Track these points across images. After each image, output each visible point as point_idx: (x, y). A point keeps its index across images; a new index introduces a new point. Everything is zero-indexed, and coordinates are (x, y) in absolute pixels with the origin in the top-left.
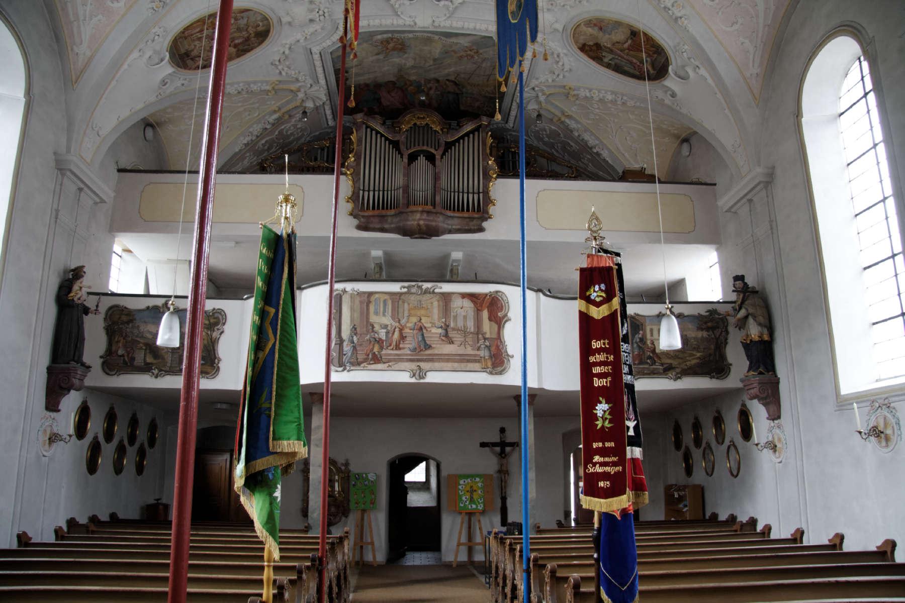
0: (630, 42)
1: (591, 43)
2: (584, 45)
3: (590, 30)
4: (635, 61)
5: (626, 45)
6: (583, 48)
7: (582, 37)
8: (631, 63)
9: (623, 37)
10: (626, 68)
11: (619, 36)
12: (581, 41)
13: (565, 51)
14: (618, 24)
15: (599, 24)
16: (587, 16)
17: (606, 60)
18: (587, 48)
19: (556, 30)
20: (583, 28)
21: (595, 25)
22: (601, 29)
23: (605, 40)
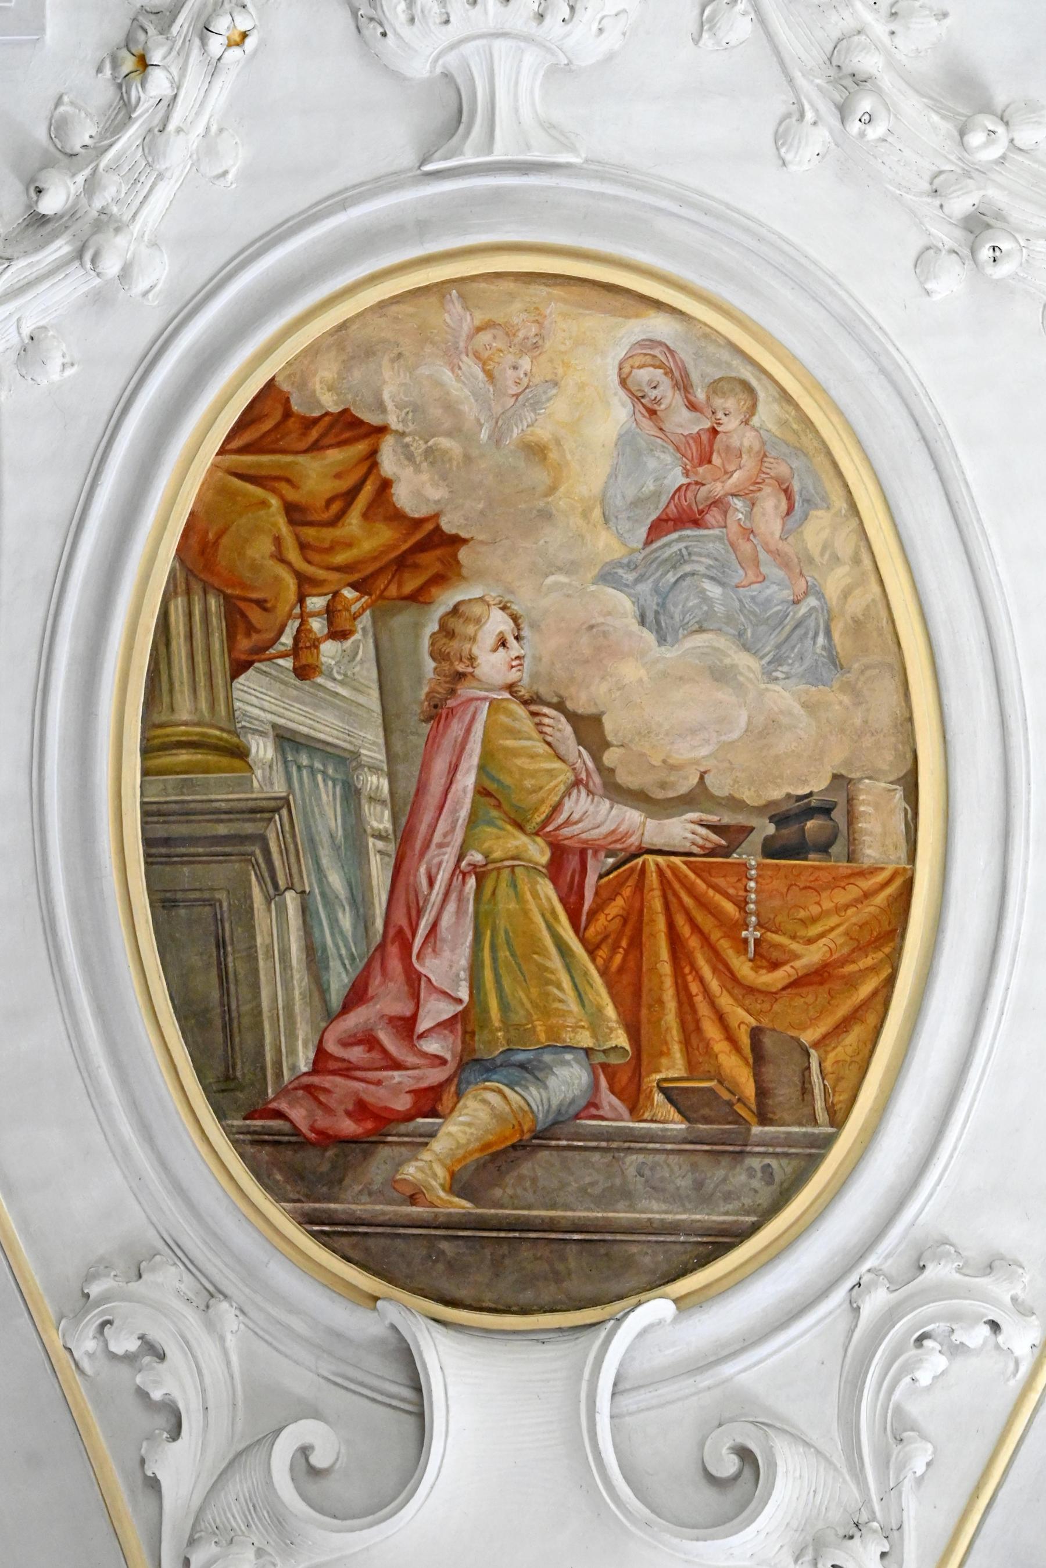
0: (680, 830)
1: (414, 490)
2: (351, 428)
3: (618, 414)
4: (446, 967)
5: (593, 817)
6: (270, 425)
7: (459, 383)
8: (399, 940)
9: (692, 753)
10: (277, 930)
11: (704, 718)
12: (389, 391)
13: (158, 275)
14: (858, 650)
15: (731, 469)
16: (790, 332)
17: (262, 698)
18: (318, 474)
19: (454, 112)
20: (597, 352)
21: (704, 449)
22: (680, 517)
23: (549, 603)
